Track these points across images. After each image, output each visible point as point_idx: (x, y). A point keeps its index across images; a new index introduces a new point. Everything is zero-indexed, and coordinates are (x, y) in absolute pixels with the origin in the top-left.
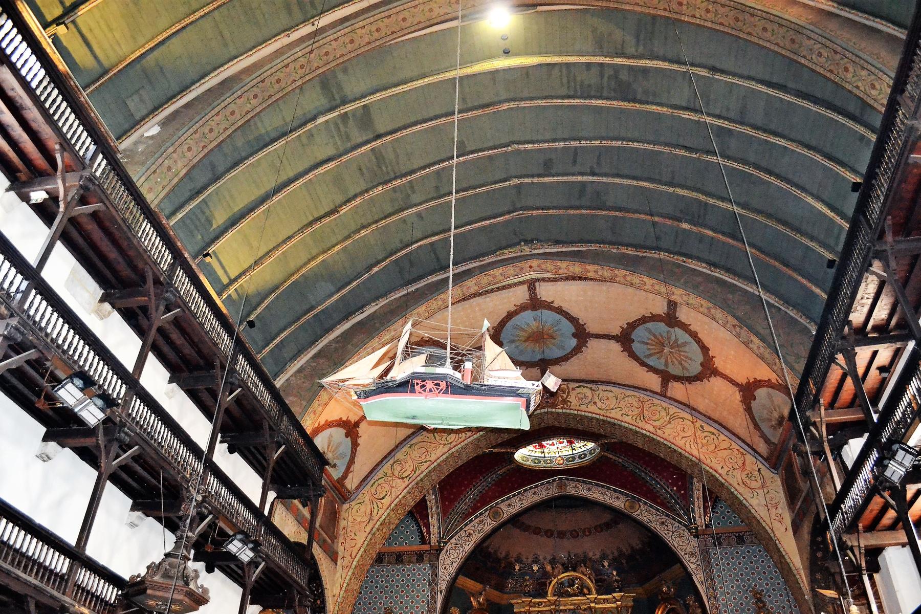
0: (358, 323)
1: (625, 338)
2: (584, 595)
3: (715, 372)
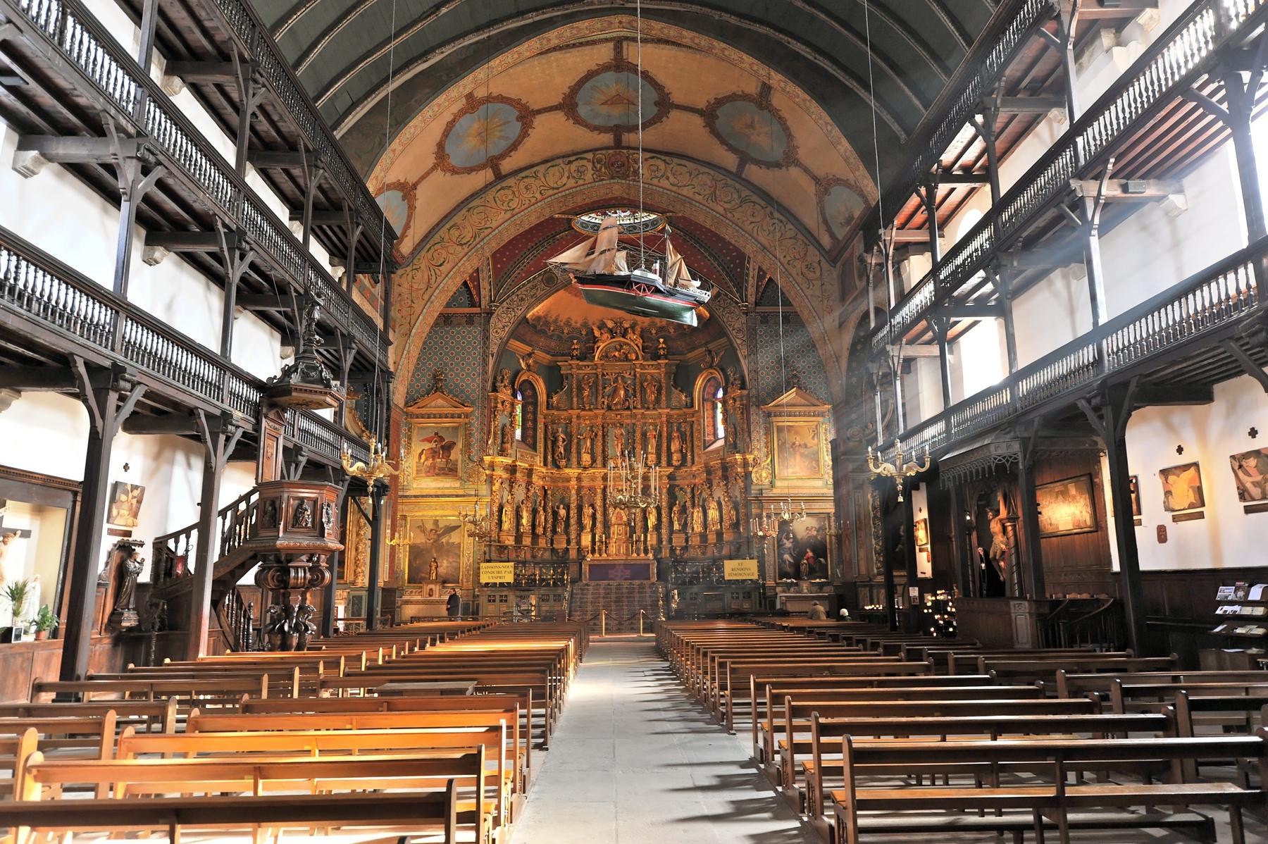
1: (709, 115)
3: (797, 163)
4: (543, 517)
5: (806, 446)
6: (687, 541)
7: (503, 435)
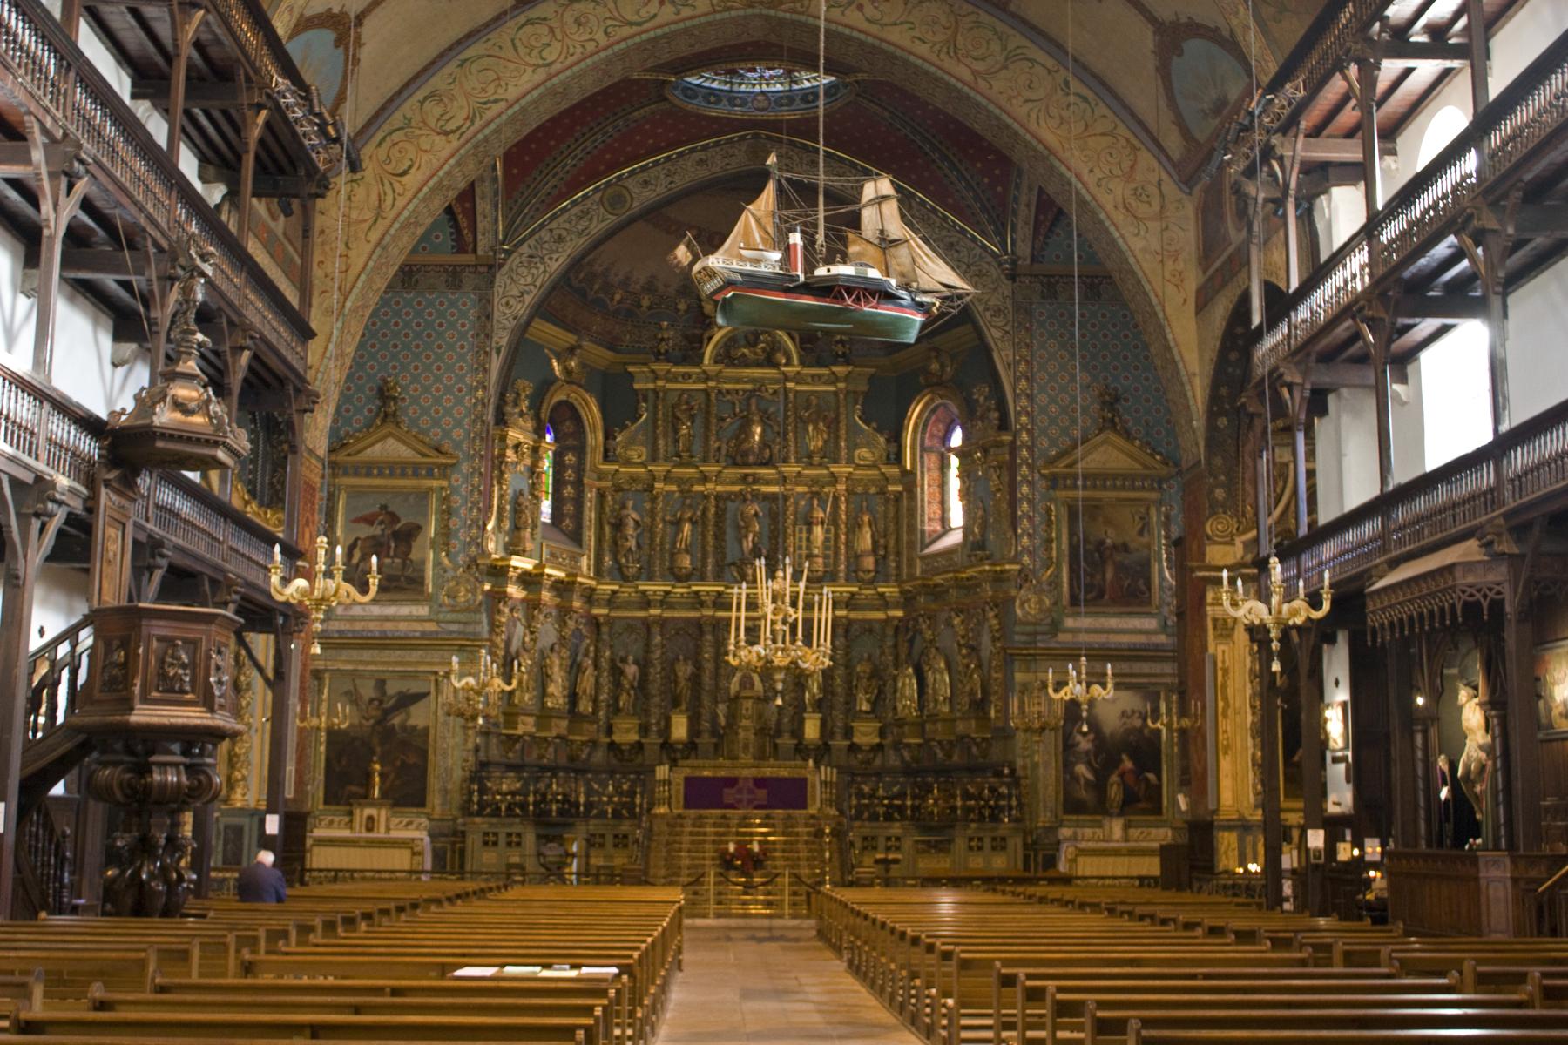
2: (776, 365)
4: (592, 680)
5: (1125, 548)
6: (882, 733)
7: (517, 510)
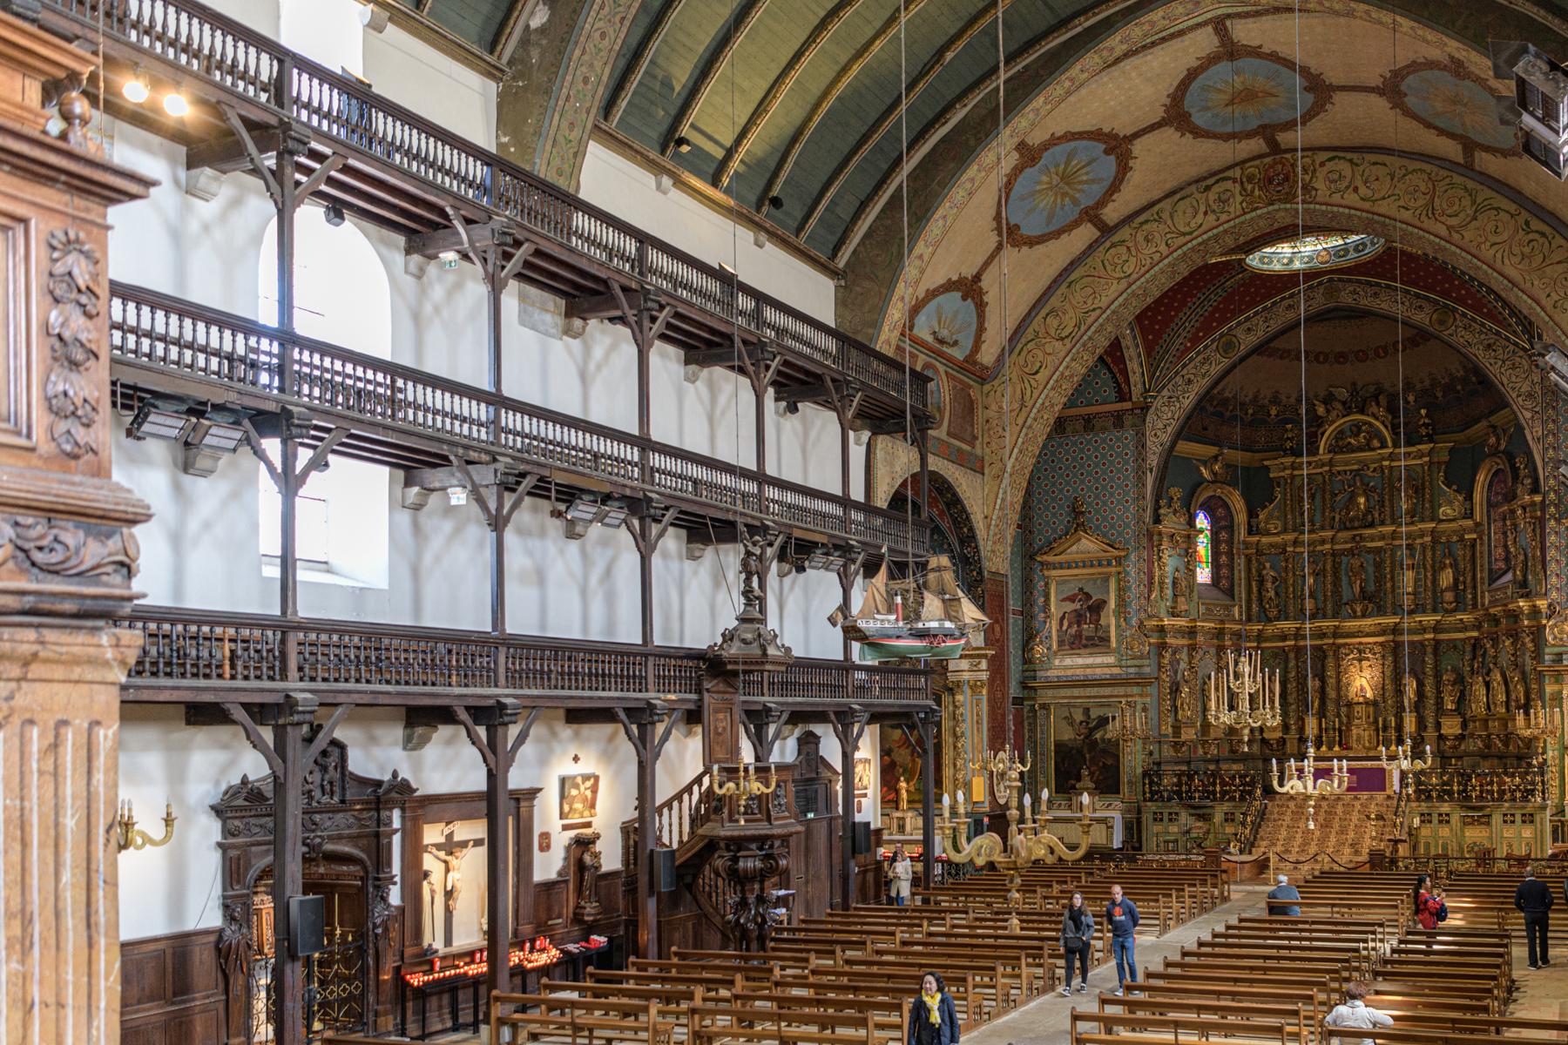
0: (942, 140)
